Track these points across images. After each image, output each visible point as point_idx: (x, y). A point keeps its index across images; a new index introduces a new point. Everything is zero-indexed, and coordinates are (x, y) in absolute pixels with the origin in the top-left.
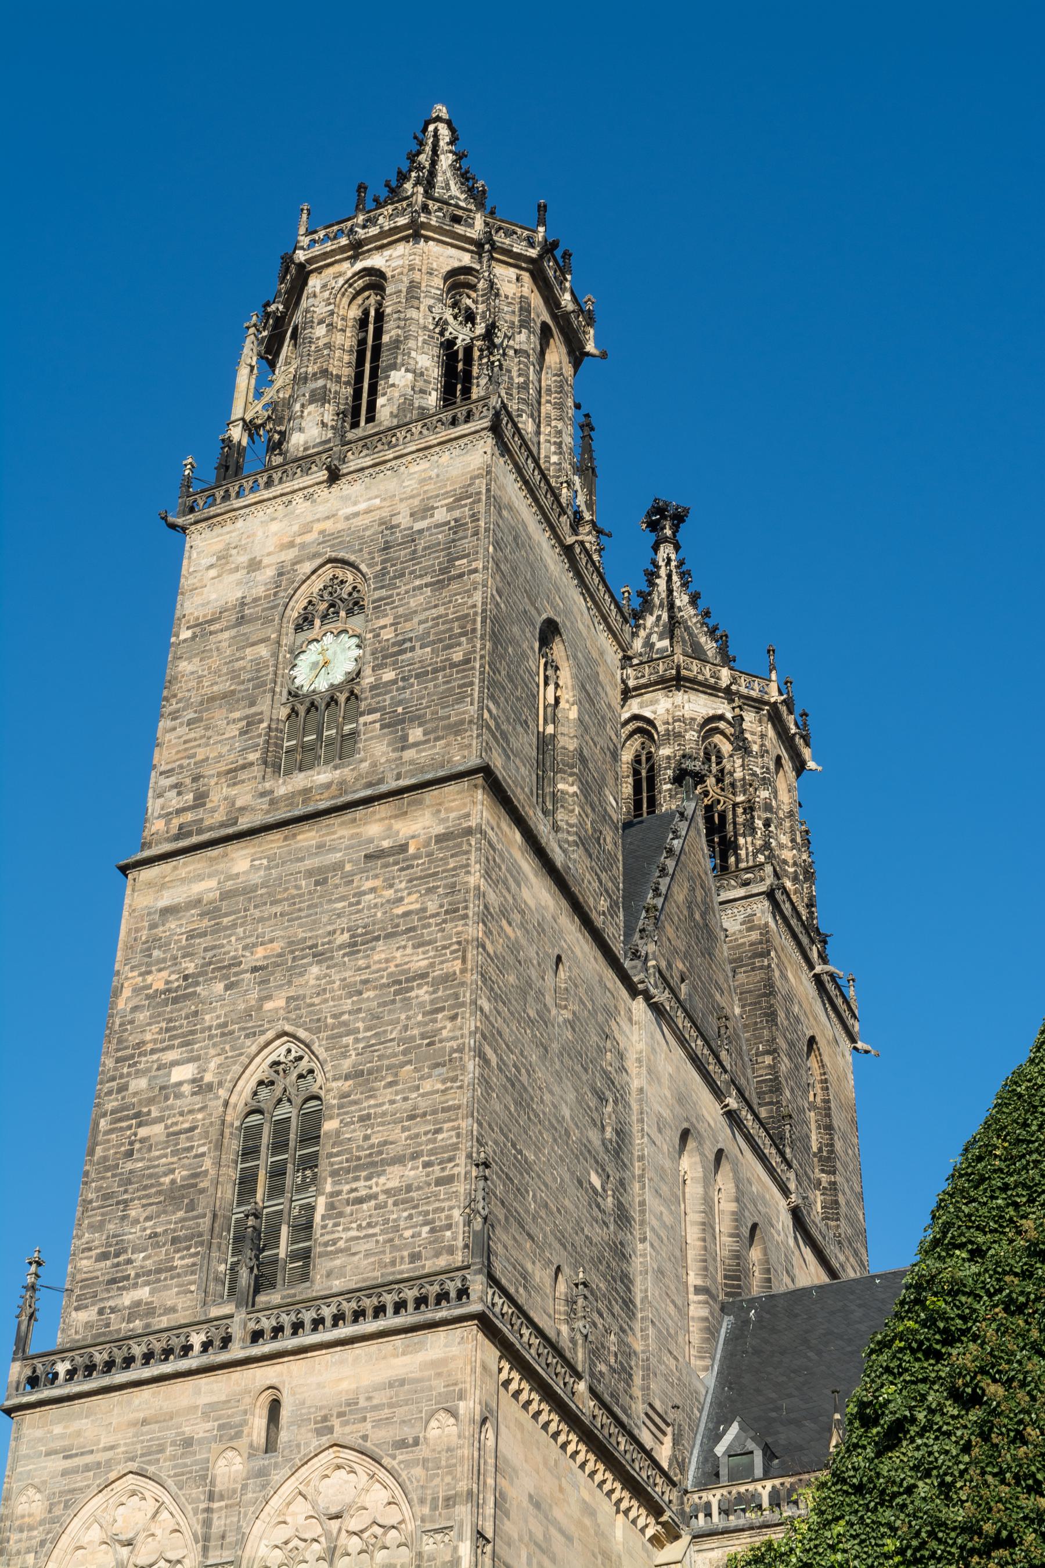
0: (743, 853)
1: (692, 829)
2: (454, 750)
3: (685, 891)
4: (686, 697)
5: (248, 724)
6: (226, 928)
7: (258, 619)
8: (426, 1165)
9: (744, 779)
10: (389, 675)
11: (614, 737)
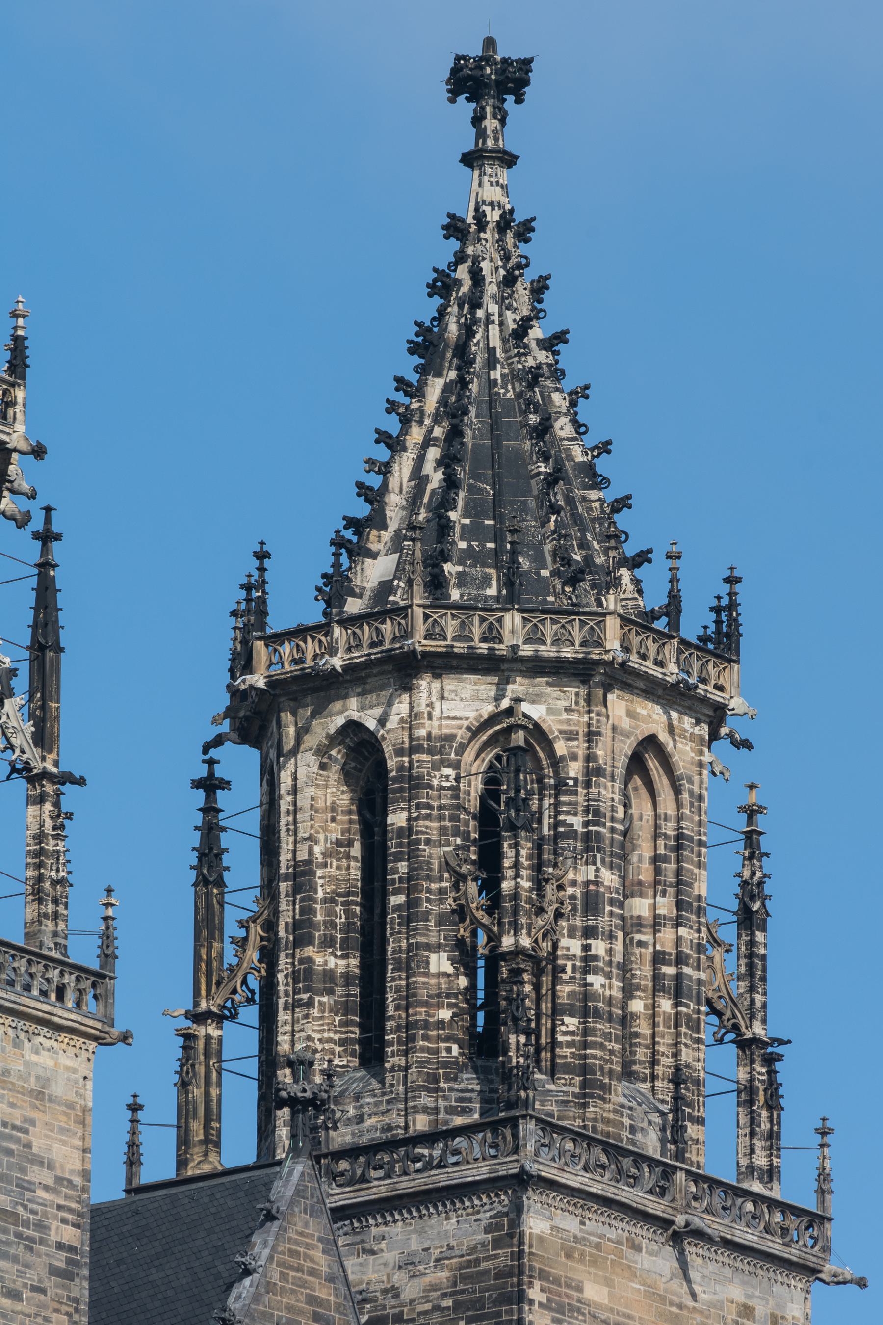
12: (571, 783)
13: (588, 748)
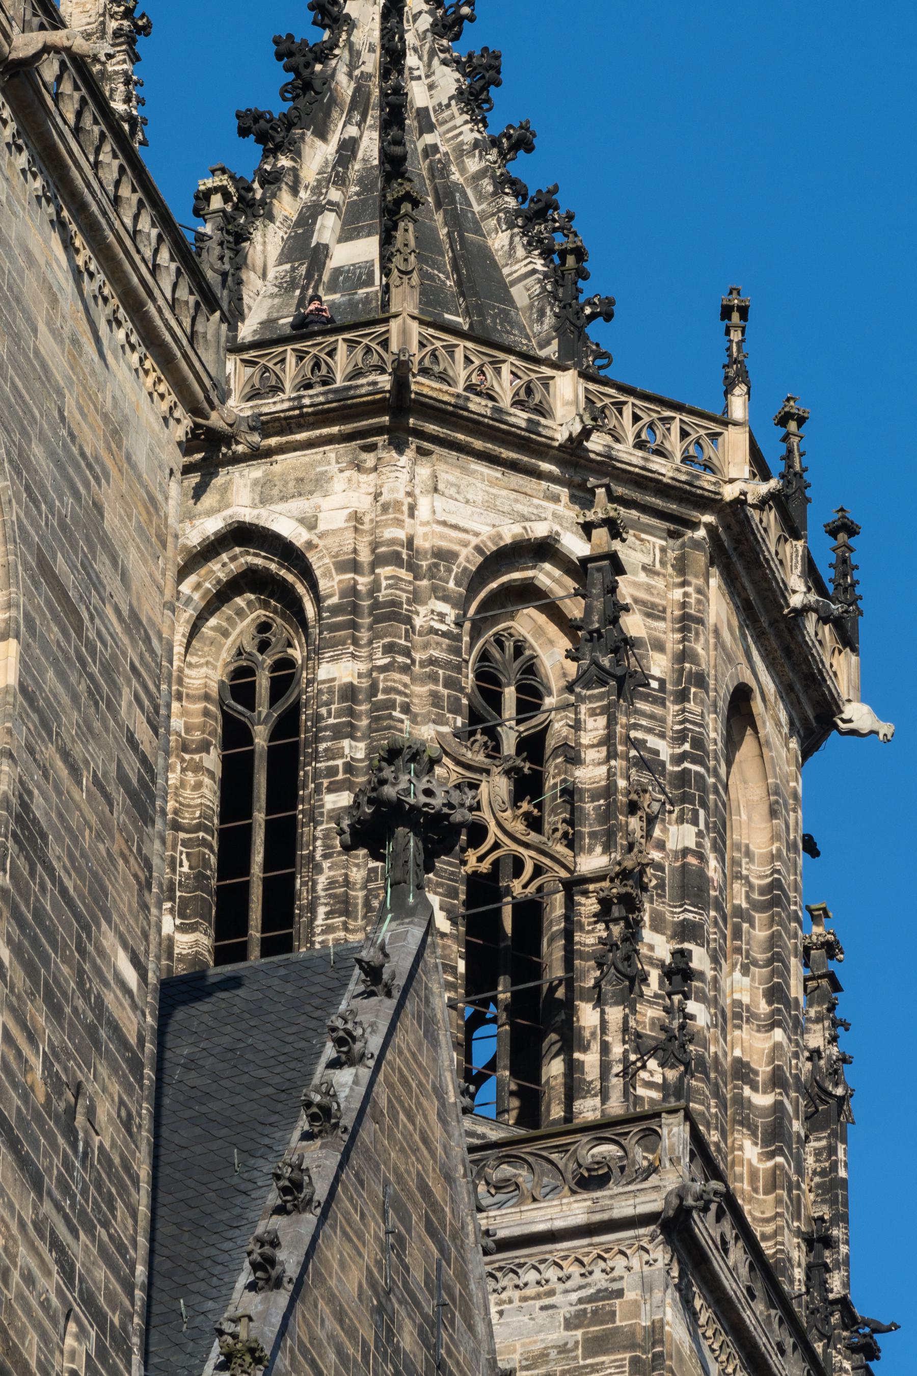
0: (590, 1059)
1: (407, 1020)
3: (371, 1252)
4: (424, 471)
9: (609, 790)
11: (143, 733)
12: (654, 684)
13: (684, 639)
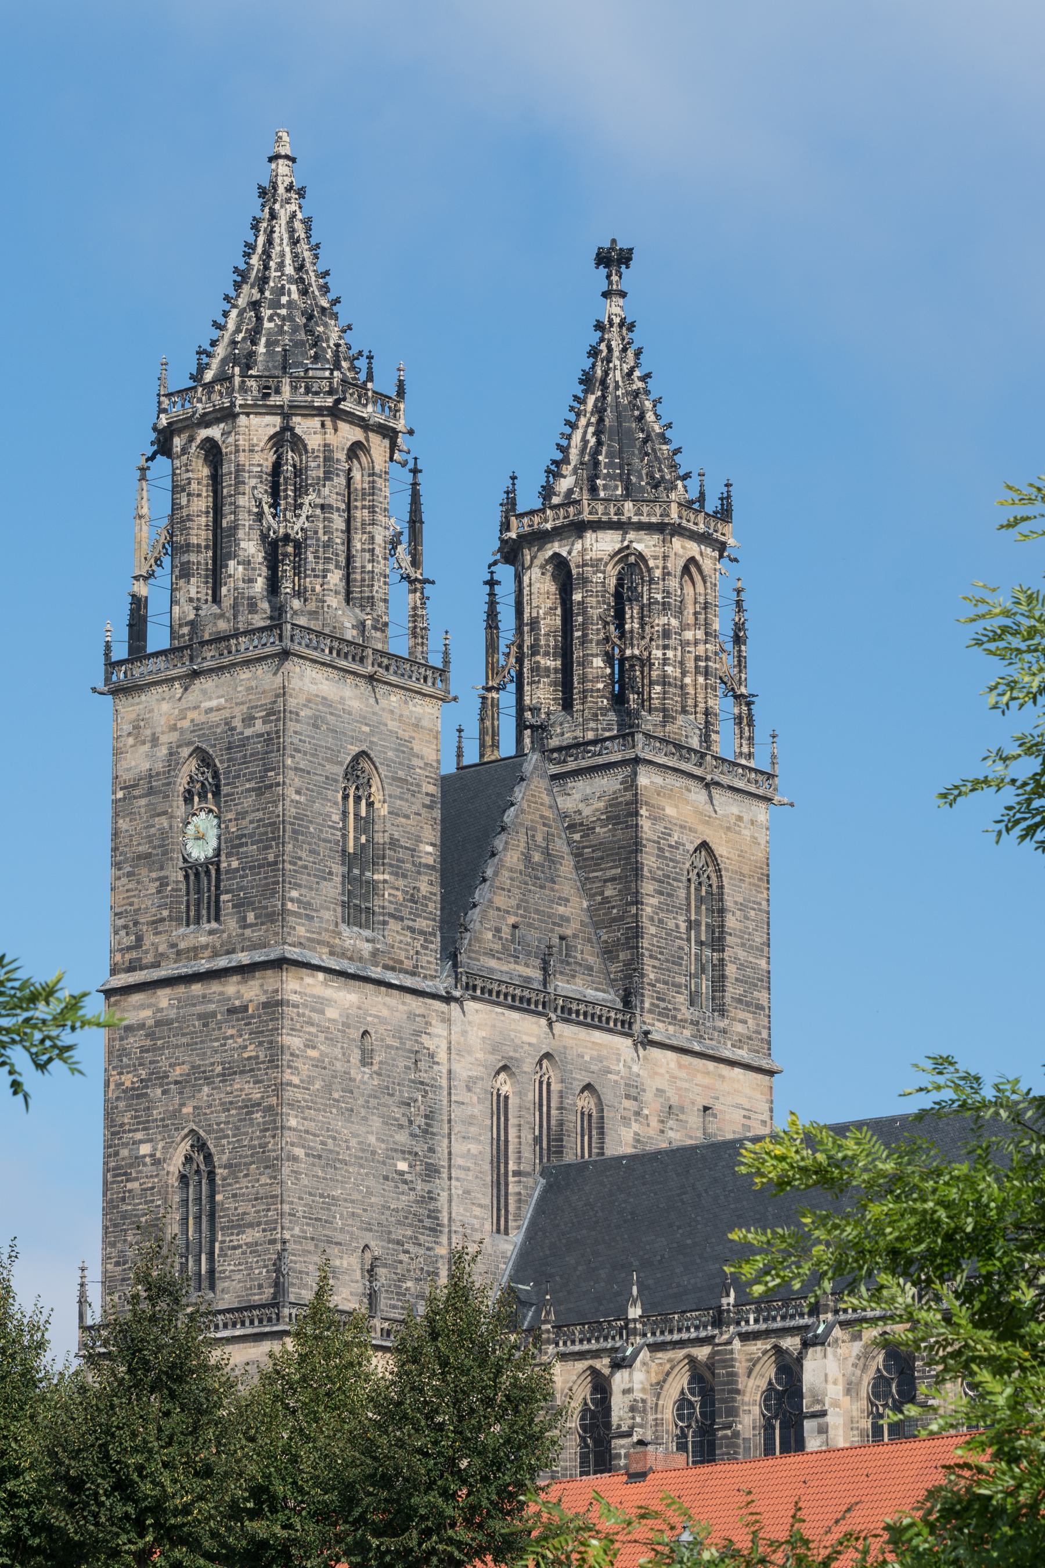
2: (270, 934)
5: (161, 885)
6: (160, 1049)
7: (160, 792)
8: (264, 1230)
10: (235, 864)
